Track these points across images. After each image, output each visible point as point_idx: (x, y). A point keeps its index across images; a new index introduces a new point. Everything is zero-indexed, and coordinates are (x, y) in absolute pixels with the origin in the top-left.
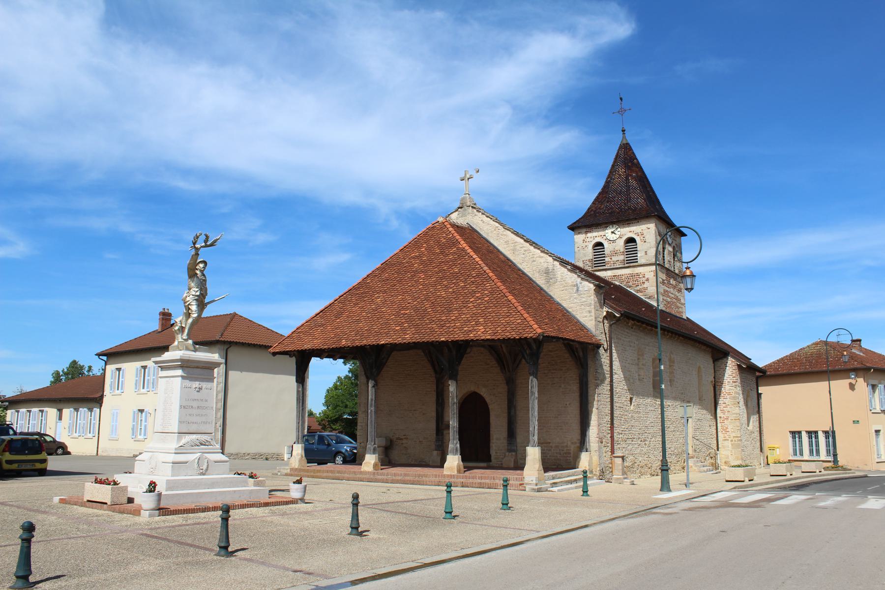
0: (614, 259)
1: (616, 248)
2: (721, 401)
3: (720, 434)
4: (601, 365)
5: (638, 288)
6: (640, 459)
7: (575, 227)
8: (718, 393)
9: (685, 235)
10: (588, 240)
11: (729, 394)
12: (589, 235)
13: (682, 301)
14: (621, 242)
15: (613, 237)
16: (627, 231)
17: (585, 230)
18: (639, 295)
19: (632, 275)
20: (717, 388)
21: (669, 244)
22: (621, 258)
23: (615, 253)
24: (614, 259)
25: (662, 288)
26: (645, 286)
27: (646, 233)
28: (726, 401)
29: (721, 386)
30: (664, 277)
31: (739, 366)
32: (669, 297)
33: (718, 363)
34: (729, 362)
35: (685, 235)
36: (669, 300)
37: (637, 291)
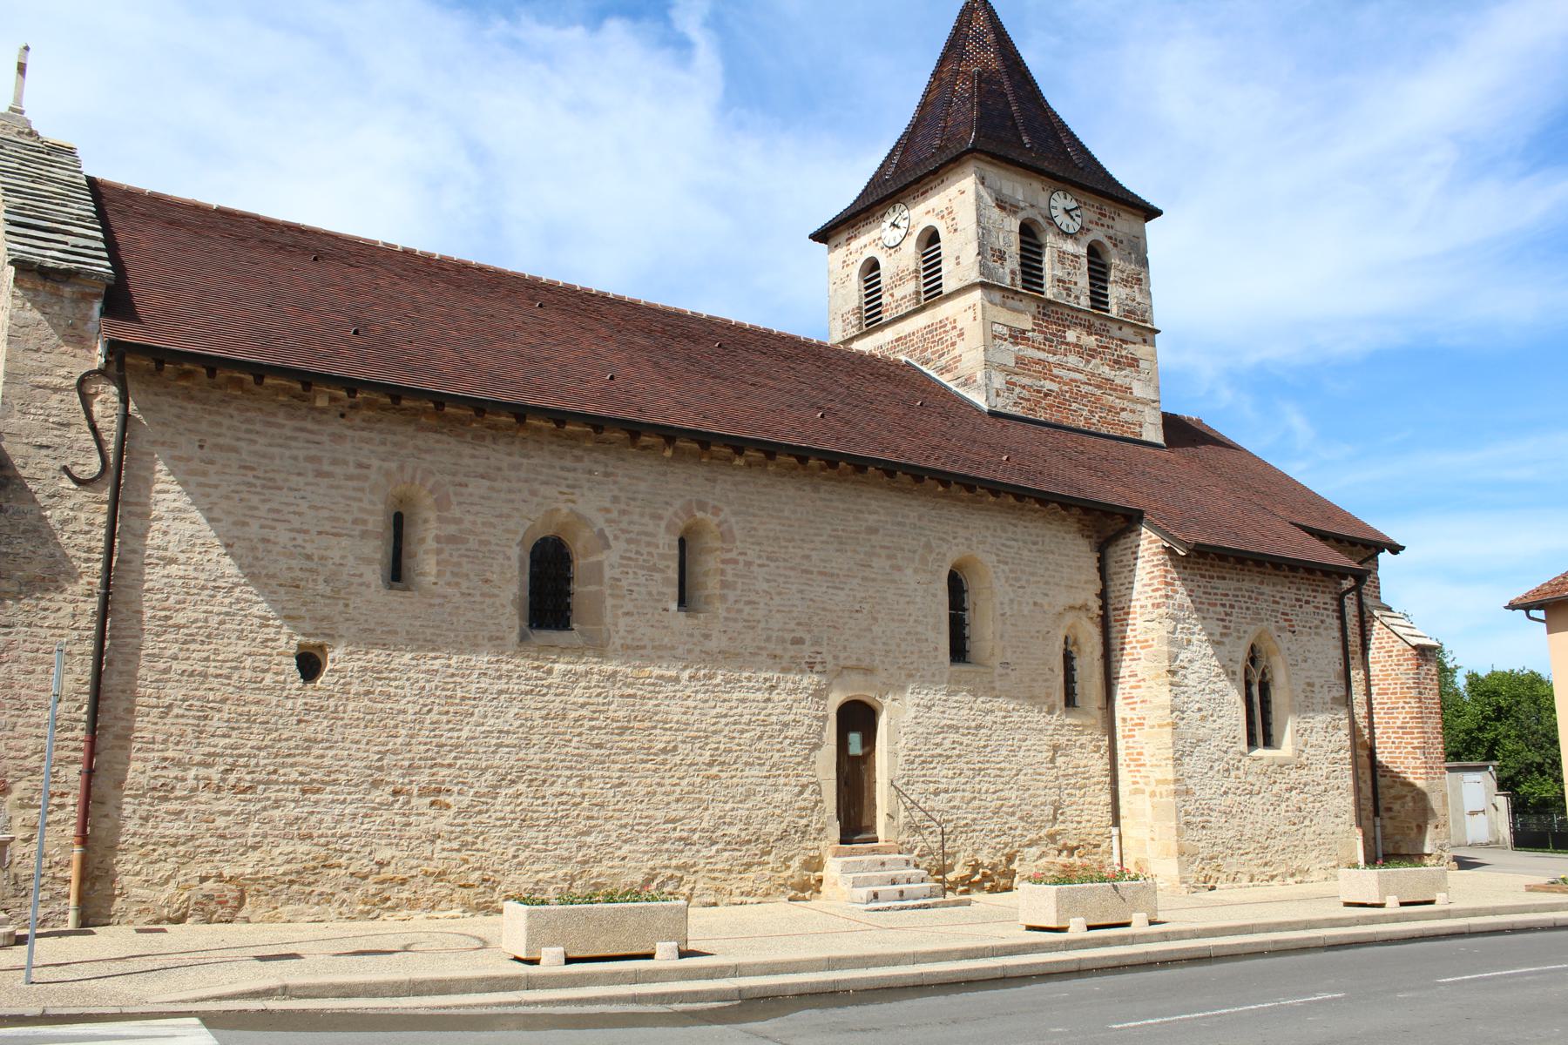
0: (898, 293)
1: (902, 266)
2: (1125, 668)
3: (1123, 773)
4: (40, 532)
5: (943, 361)
6: (384, 854)
7: (823, 236)
8: (1116, 643)
9: (1156, 213)
10: (852, 258)
11: (1145, 644)
12: (855, 244)
13: (1139, 390)
14: (910, 246)
15: (891, 240)
16: (920, 214)
17: (845, 236)
18: (943, 379)
19: (931, 329)
20: (1115, 628)
21: (1067, 235)
22: (910, 287)
23: (900, 279)
24: (898, 293)
25: (1008, 353)
26: (956, 352)
27: (957, 206)
28: (1138, 667)
29: (1124, 622)
30: (1026, 322)
31: (1169, 551)
32: (1053, 378)
33: (1115, 552)
34: (1144, 544)
35: (1156, 213)
36: (1048, 385)
37: (943, 370)
